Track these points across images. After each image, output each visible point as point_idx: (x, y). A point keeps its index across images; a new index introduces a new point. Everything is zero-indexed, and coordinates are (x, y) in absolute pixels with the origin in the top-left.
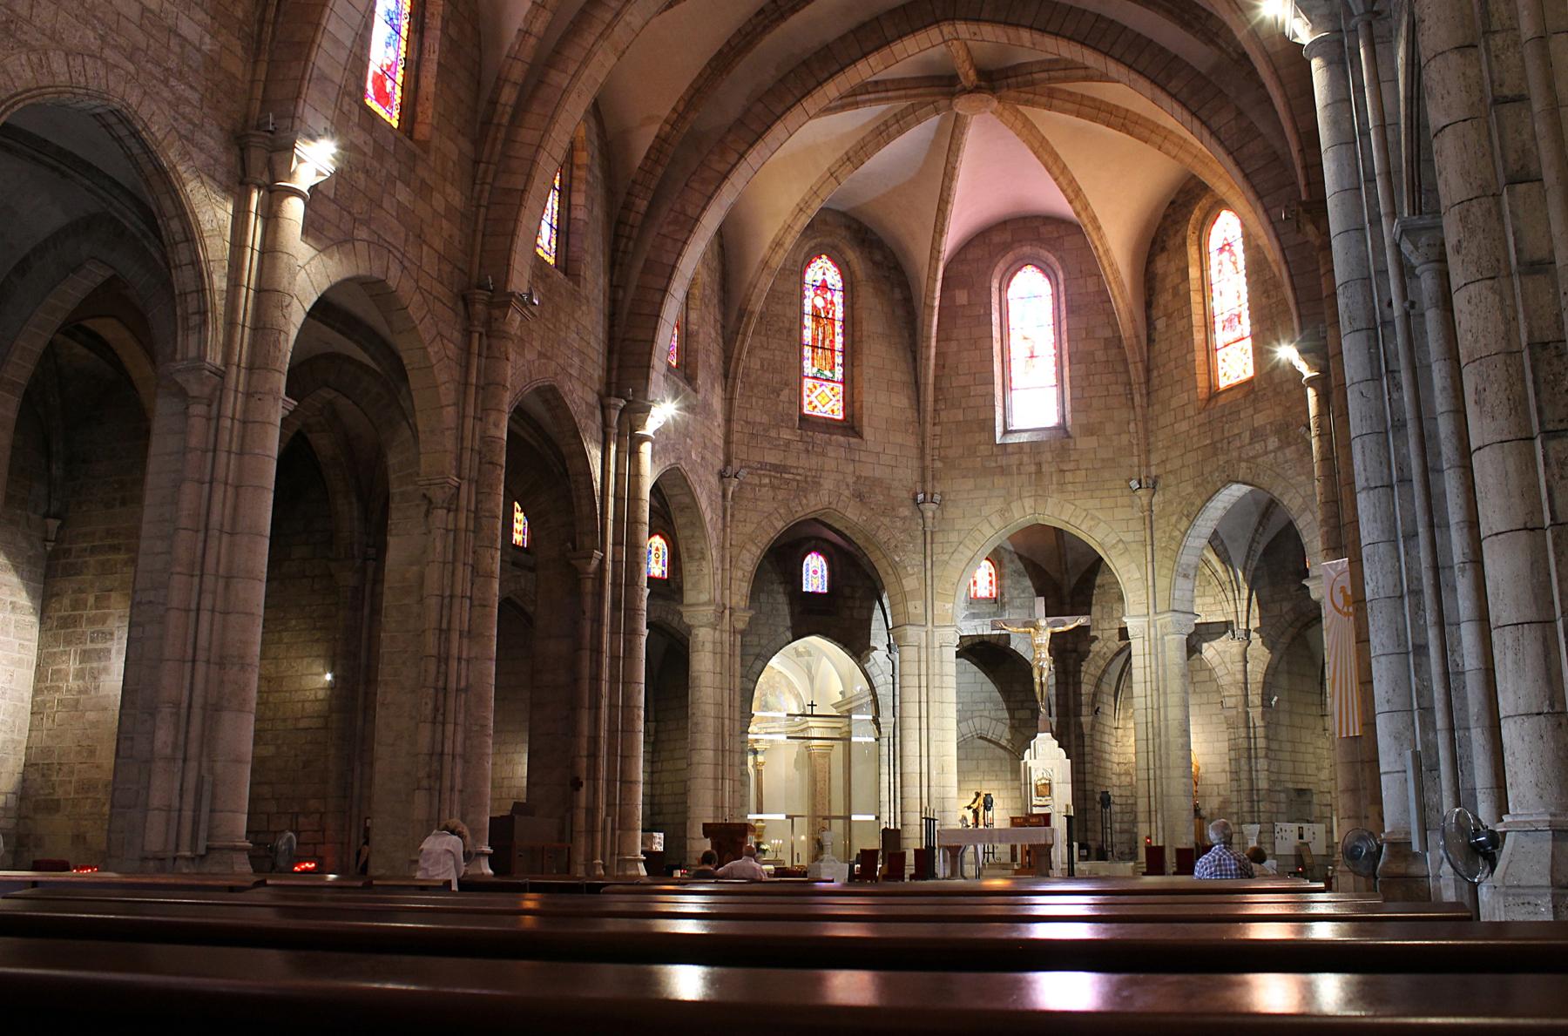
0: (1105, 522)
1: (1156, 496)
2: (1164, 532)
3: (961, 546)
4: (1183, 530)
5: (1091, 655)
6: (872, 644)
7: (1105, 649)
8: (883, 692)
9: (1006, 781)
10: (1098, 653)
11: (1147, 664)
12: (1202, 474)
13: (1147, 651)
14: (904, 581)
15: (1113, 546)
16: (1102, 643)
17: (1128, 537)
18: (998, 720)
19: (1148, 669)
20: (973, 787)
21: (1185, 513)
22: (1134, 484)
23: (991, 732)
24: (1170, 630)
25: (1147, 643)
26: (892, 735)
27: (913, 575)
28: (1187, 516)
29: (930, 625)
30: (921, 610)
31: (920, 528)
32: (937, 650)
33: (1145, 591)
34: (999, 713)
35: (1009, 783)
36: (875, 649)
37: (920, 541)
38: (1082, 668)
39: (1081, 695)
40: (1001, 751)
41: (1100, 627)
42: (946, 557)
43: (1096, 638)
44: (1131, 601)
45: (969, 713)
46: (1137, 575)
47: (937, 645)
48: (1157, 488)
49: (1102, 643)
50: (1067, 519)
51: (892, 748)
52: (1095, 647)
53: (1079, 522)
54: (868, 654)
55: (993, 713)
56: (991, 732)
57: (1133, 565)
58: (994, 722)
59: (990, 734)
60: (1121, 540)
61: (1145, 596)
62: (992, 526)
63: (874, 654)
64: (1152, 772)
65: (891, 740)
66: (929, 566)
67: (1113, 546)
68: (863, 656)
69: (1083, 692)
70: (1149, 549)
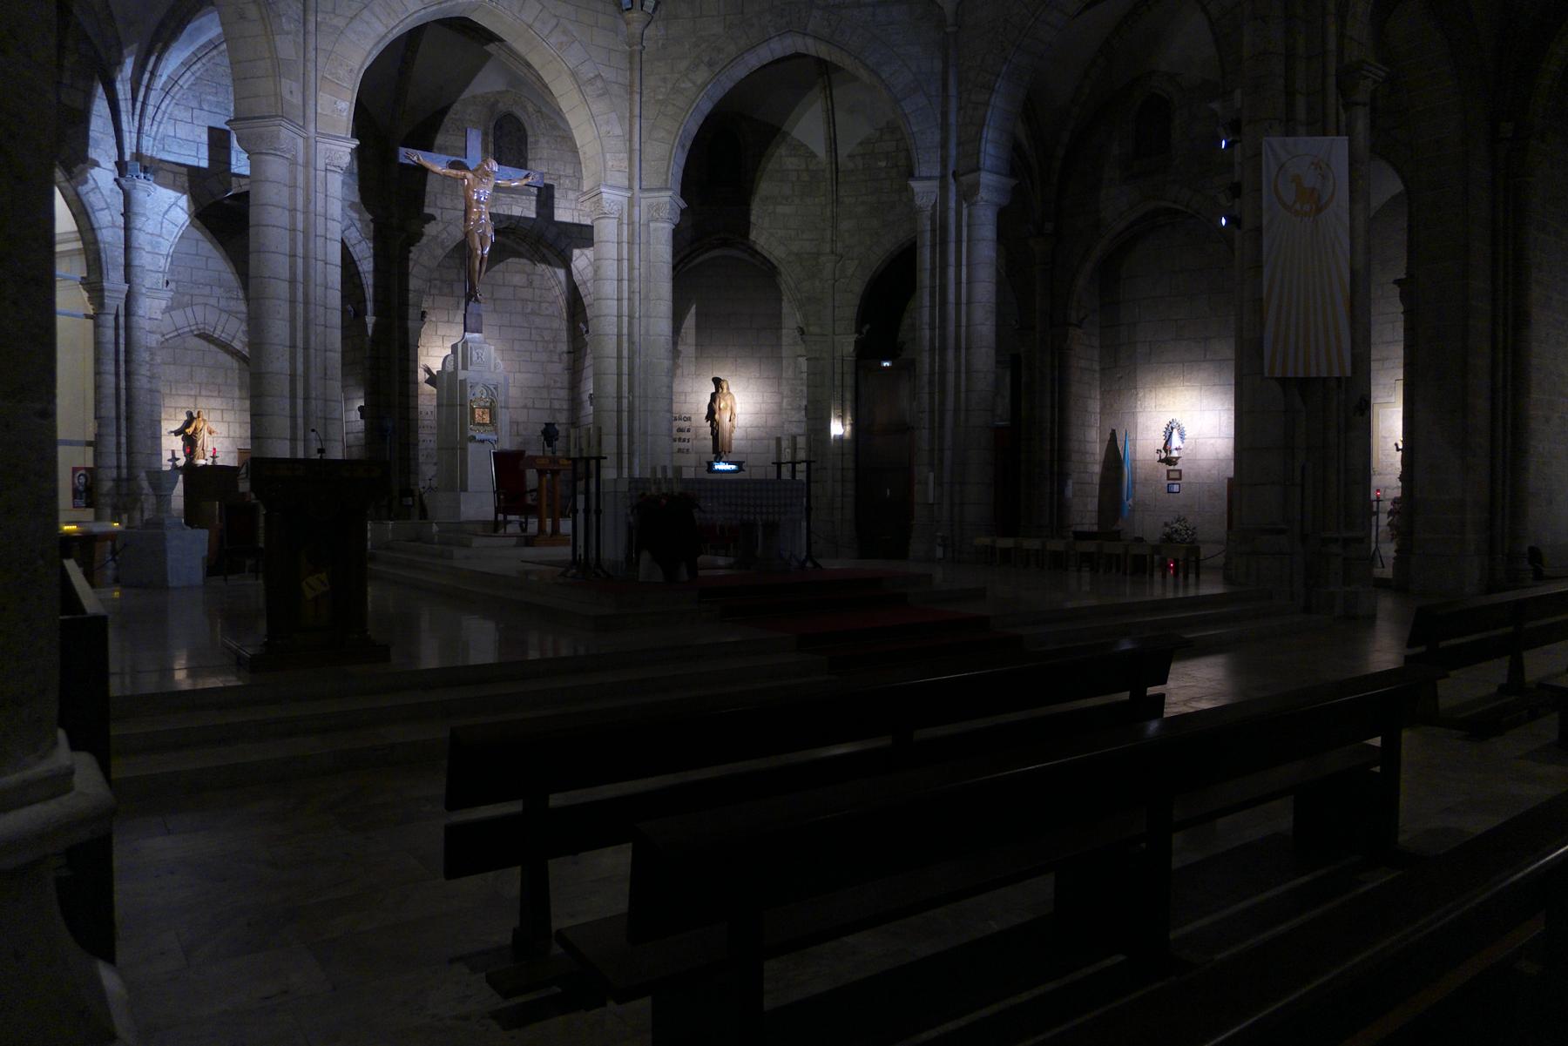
0: (579, 42)
1: (652, 26)
2: (665, 80)
3: (365, 12)
4: (699, 82)
5: (424, 240)
6: (93, 153)
7: (445, 235)
8: (109, 239)
10: (435, 238)
11: (625, 256)
12: (742, 13)
13: (625, 237)
14: (277, 38)
15: (591, 81)
16: (441, 226)
17: (607, 74)
19: (625, 263)
21: (706, 59)
24: (665, 213)
25: (625, 227)
26: (122, 312)
28: (710, 65)
29: (312, 128)
30: (297, 100)
32: (321, 174)
34: (232, 303)
36: (96, 164)
38: (411, 255)
39: (407, 290)
40: (228, 358)
41: (438, 203)
42: (340, 22)
43: (431, 218)
44: (610, 163)
46: (618, 131)
47: (321, 164)
48: (656, 16)
49: (441, 226)
50: (530, 21)
51: (122, 332)
52: (430, 229)
54: (84, 171)
60: (598, 76)
61: (626, 163)
63: (95, 172)
64: (625, 402)
65: (122, 320)
66: (311, 27)
67: (591, 81)
68: (75, 170)
69: (411, 287)
70: (637, 97)
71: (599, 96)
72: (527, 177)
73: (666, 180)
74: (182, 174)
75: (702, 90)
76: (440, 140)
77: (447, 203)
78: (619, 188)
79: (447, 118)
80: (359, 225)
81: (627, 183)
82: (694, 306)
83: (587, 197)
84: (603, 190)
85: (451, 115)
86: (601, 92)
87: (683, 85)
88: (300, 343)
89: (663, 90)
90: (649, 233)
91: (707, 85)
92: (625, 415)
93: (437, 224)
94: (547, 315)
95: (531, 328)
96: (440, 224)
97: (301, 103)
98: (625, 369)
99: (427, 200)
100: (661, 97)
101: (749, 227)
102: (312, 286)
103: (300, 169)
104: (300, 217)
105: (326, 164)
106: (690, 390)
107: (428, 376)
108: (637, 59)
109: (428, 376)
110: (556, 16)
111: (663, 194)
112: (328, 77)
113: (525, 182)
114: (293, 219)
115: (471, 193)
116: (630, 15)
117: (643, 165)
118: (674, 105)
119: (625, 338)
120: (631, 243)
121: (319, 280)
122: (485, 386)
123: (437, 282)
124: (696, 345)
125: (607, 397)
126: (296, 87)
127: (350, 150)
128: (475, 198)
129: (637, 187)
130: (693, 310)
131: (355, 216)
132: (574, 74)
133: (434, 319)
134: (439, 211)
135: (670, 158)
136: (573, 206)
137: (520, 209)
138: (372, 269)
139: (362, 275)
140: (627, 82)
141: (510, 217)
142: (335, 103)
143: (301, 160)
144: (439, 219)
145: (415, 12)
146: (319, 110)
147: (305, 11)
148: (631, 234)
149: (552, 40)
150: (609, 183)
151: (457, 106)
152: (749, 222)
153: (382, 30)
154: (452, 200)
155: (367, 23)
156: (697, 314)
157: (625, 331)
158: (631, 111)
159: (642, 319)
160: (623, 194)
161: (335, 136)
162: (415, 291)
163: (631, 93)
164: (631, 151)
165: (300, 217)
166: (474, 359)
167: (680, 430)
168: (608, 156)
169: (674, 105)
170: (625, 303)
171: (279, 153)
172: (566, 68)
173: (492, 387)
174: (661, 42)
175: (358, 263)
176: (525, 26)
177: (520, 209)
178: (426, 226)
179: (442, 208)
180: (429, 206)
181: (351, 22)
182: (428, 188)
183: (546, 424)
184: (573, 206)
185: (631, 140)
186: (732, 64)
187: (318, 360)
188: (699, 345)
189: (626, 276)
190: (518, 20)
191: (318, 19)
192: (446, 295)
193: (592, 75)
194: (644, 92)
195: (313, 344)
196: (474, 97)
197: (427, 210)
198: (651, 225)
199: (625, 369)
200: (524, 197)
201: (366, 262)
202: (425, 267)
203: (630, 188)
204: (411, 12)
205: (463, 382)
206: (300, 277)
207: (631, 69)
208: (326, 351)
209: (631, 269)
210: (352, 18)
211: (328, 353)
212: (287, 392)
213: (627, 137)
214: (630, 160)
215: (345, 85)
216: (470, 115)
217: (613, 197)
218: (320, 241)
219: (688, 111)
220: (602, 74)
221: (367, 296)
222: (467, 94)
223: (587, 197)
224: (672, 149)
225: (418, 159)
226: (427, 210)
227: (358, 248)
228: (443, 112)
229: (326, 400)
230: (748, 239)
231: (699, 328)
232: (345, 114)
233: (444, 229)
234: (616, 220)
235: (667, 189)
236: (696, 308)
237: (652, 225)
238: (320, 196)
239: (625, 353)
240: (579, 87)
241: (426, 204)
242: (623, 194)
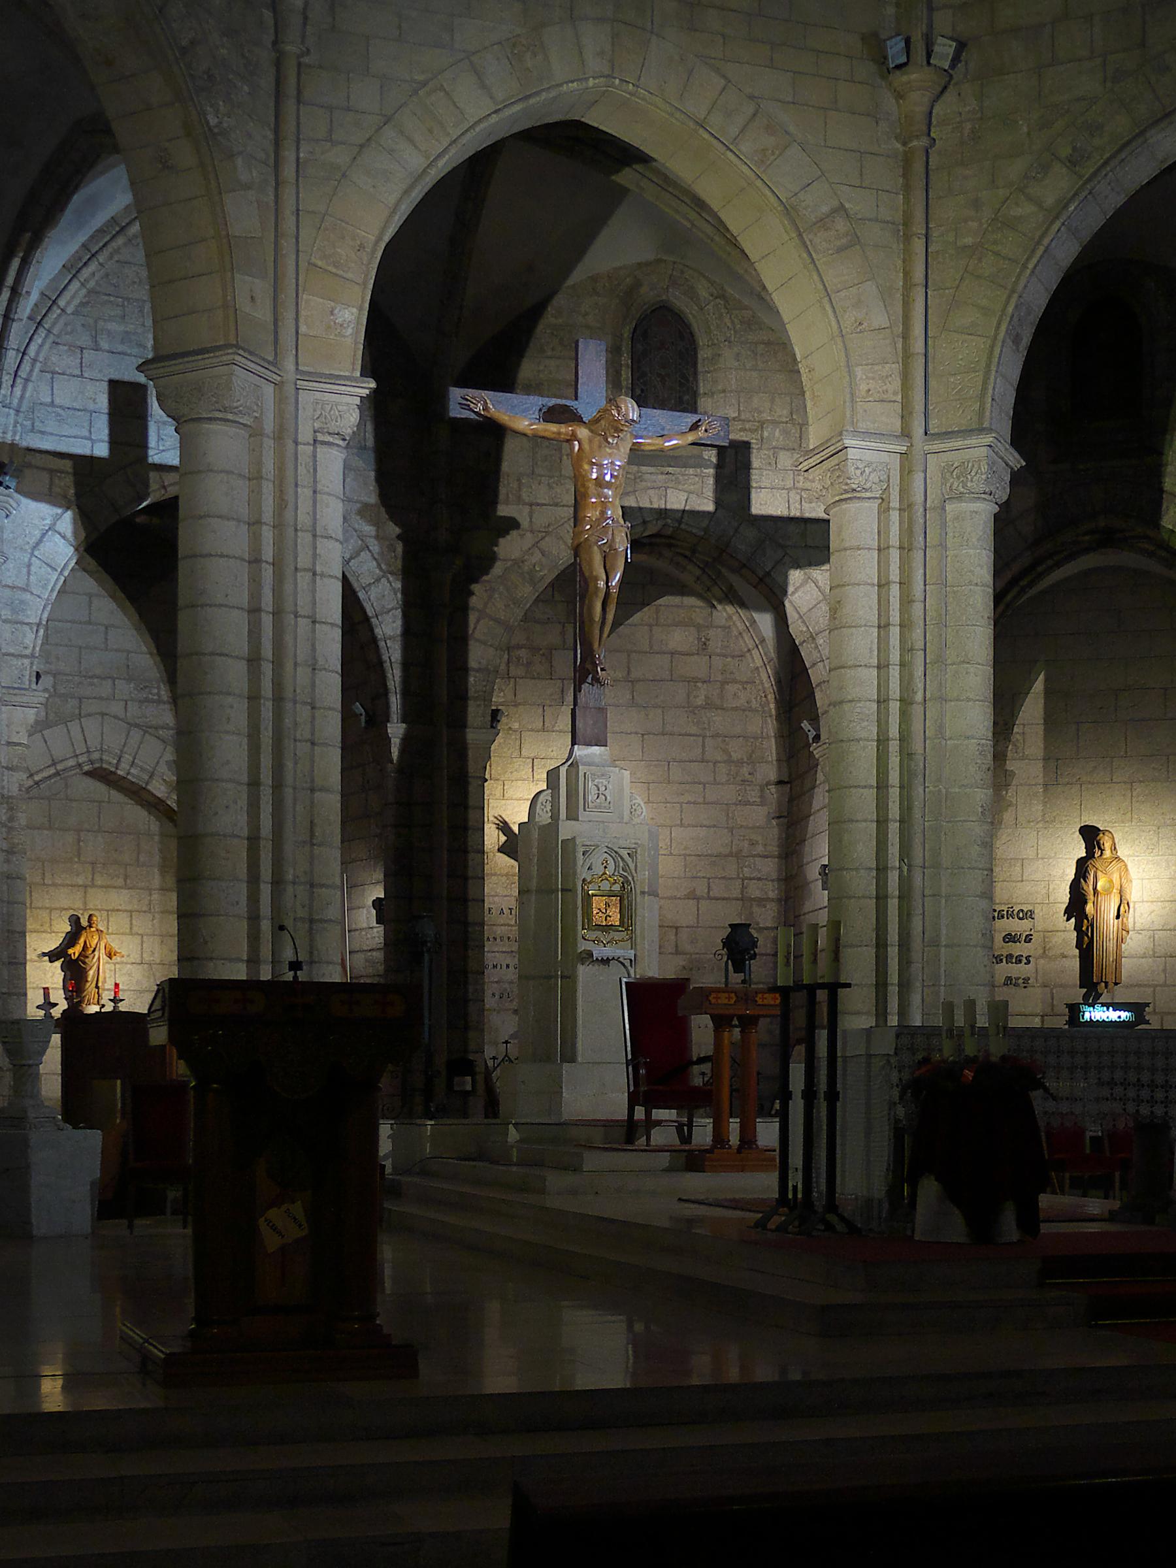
1: (950, 96)
2: (976, 204)
4: (1050, 201)
5: (498, 569)
9: (150, 890)
11: (895, 575)
13: (894, 539)
15: (822, 223)
16: (529, 539)
18: (147, 729)
19: (895, 590)
20: (65, 903)
22: (895, 50)
23: (128, 758)
24: (977, 483)
25: (895, 516)
27: (247, 187)
29: (290, 365)
30: (263, 314)
31: (268, 38)
32: (305, 450)
33: (896, 368)
35: (156, 896)
37: (266, 82)
38: (474, 601)
39: (464, 669)
41: (525, 496)
43: (512, 524)
44: (863, 387)
45: (72, 703)
46: (880, 319)
47: (305, 434)
49: (529, 539)
52: (509, 547)
53: (734, 130)
55: (133, 709)
56: (128, 758)
57: (870, 288)
58: (136, 734)
59: (124, 765)
61: (896, 384)
62: (483, 86)
64: (893, 878)
66: (289, 171)
67: (822, 223)
69: (473, 664)
70: (919, 245)
71: (840, 250)
72: (695, 427)
73: (981, 413)
74: (62, 472)
75: (1057, 217)
76: (527, 370)
77: (541, 494)
78: (880, 435)
79: (540, 327)
80: (375, 547)
81: (898, 424)
82: (1042, 677)
83: (817, 459)
84: (847, 442)
85: (549, 318)
86: (844, 241)
87: (1017, 211)
88: (266, 777)
89: (974, 225)
90: (944, 525)
91: (1066, 206)
92: (893, 904)
93: (522, 536)
94: (735, 709)
95: (704, 737)
96: (529, 535)
97: (269, 318)
98: (894, 811)
99: (503, 491)
100: (969, 240)
101: (1160, 505)
102: (289, 666)
103: (269, 443)
104: (267, 534)
105: (315, 432)
106: (1031, 853)
107: (503, 838)
108: (918, 167)
109: (503, 838)
110: (751, 97)
111: (973, 441)
112: (320, 263)
113: (691, 438)
114: (256, 539)
115: (586, 467)
116: (905, 78)
117: (932, 383)
118: (997, 254)
119: (894, 746)
120: (905, 549)
121: (302, 654)
122: (611, 851)
123: (523, 653)
124: (1046, 759)
125: (857, 869)
126: (261, 287)
127: (357, 401)
128: (594, 476)
129: (918, 430)
130: (1039, 685)
131: (369, 529)
132: (789, 212)
133: (516, 726)
134: (527, 509)
135: (988, 366)
136: (789, 484)
137: (683, 496)
138: (399, 632)
139: (382, 644)
140: (899, 216)
141: (663, 513)
142: (332, 313)
143: (269, 425)
144: (525, 523)
145: (480, 121)
146: (303, 329)
147: (277, 144)
148: (907, 531)
149: (746, 147)
150: (862, 426)
151: (559, 300)
152: (1161, 491)
153: (416, 161)
154: (550, 486)
155: (391, 152)
156: (1048, 692)
157: (894, 731)
158: (907, 274)
159: (928, 704)
160: (891, 447)
161: (331, 376)
162: (478, 670)
163: (907, 238)
164: (907, 356)
165: (267, 534)
166: (591, 797)
167: (1010, 938)
168: (859, 372)
169: (997, 254)
170: (895, 672)
171: (230, 416)
172: (773, 199)
173: (624, 853)
174: (968, 126)
175: (374, 621)
176: (691, 124)
177: (683, 496)
178: (502, 541)
179: (531, 505)
180: (507, 503)
181: (359, 153)
182: (505, 466)
183: (730, 925)
184: (789, 484)
185: (906, 336)
186: (1123, 155)
187: (299, 808)
188: (1054, 761)
189: (895, 617)
190: (678, 115)
191: (302, 155)
192: (539, 677)
193: (825, 209)
194: (935, 234)
195: (289, 779)
196: (594, 279)
197: (503, 510)
198: (948, 507)
199: (894, 811)
200: (691, 471)
201: (388, 618)
202: (497, 621)
203: (906, 434)
204: (472, 121)
205: (569, 844)
206: (267, 650)
207: (907, 188)
208: (312, 790)
209: (906, 601)
210: (362, 146)
211: (317, 794)
212: (242, 870)
213: (899, 329)
214: (906, 376)
215: (350, 275)
216: (587, 314)
217: (869, 456)
218: (303, 579)
219: (1025, 266)
220: (847, 206)
221: (390, 684)
222: (578, 275)
223: (817, 459)
224: (992, 347)
225: (486, 409)
226: (503, 510)
227: (374, 592)
228: (536, 312)
229: (312, 885)
230: (1157, 525)
231: (1051, 722)
232: (350, 331)
233: (536, 544)
234: (875, 505)
235: (981, 430)
236: (1046, 680)
237: (949, 507)
238: (305, 493)
239: (894, 777)
240: (800, 235)
241: (502, 497)
242: (891, 447)
